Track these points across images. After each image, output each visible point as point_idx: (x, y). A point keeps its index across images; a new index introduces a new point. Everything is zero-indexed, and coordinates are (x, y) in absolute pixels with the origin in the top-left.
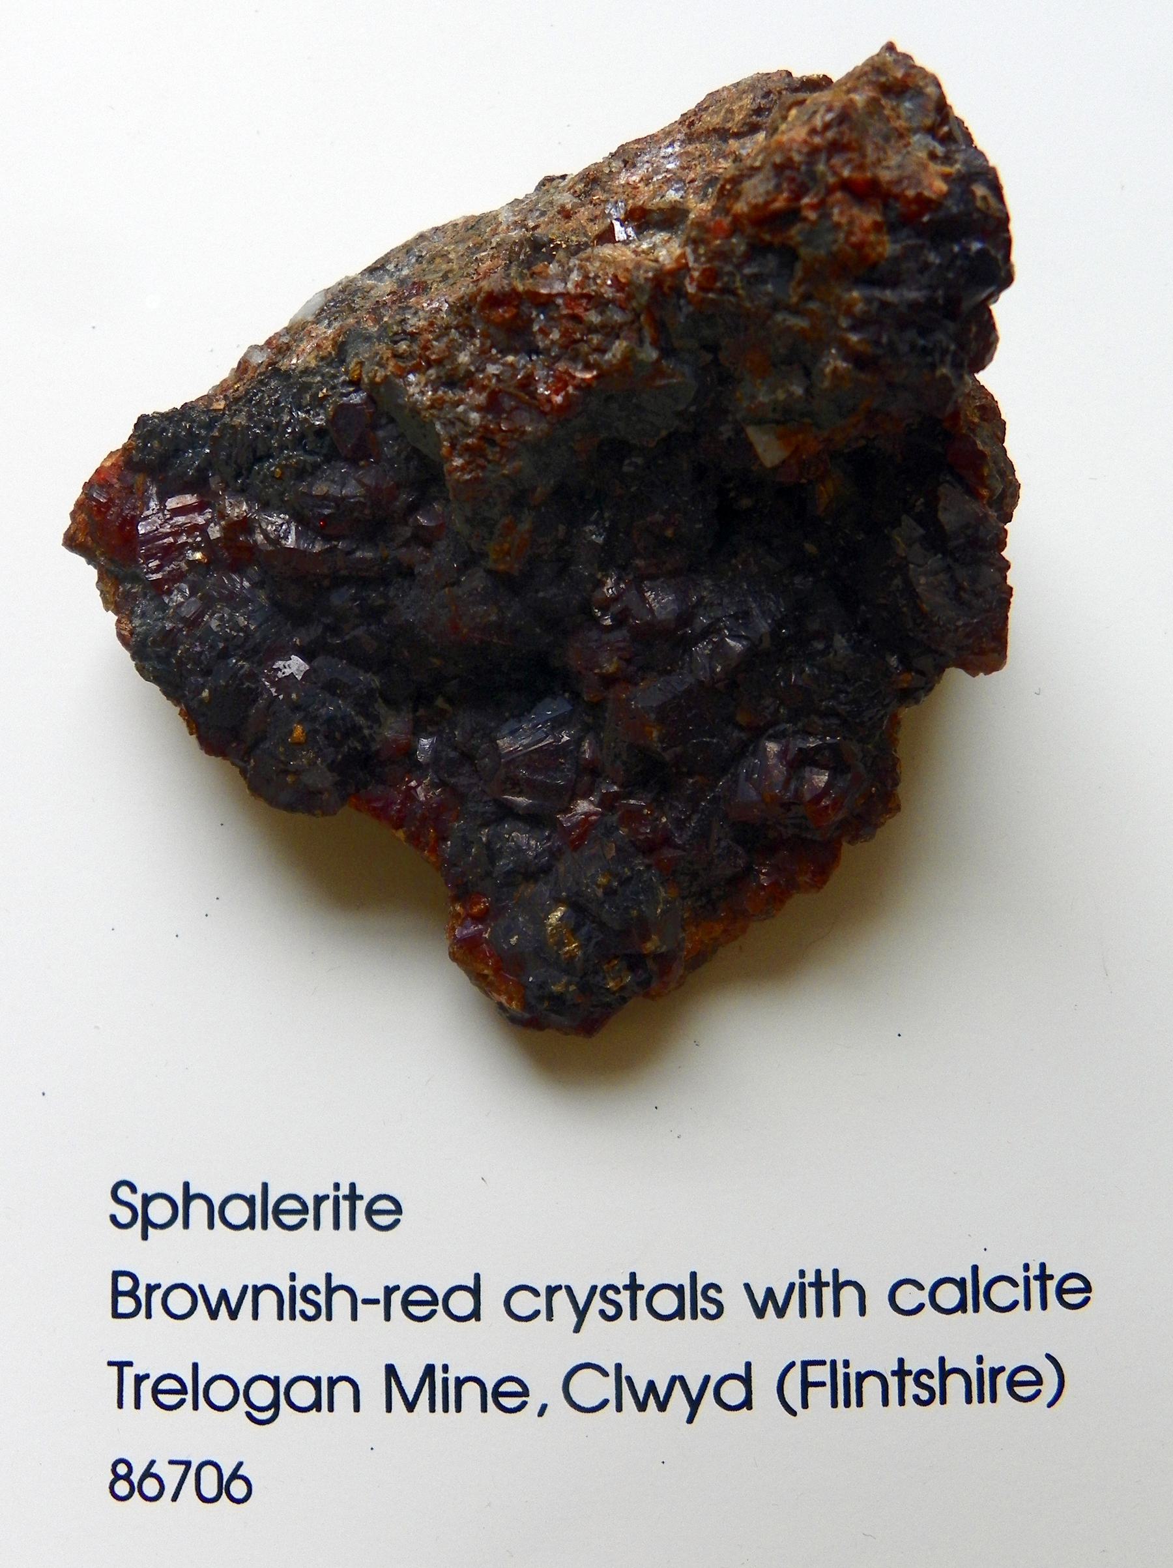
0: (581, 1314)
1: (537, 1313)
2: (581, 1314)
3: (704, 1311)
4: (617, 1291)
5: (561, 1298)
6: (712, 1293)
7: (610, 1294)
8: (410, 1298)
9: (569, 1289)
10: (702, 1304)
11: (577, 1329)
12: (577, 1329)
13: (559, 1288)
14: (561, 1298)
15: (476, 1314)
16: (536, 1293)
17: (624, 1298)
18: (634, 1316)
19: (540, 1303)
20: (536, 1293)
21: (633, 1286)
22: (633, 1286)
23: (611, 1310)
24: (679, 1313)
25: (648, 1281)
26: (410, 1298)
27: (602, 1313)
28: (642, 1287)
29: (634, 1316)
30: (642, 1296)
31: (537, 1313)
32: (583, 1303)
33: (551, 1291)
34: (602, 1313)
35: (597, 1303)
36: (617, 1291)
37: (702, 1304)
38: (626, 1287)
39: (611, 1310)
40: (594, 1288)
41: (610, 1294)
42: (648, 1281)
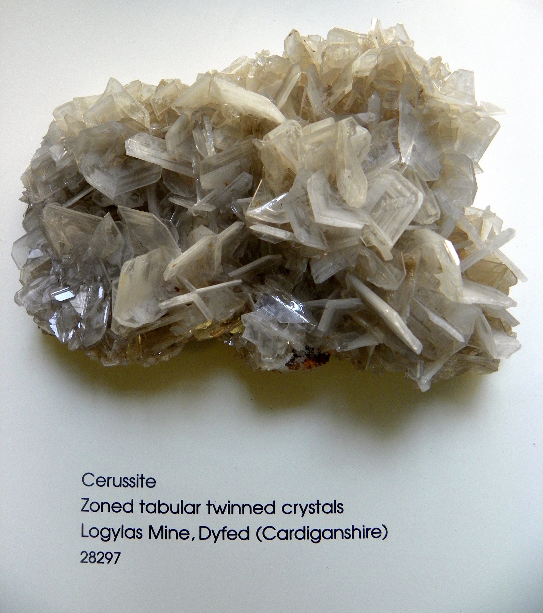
0: (304, 512)
1: (291, 512)
2: (304, 512)
3: (338, 511)
5: (298, 507)
6: (340, 506)
7: (312, 506)
9: (300, 505)
10: (337, 509)
11: (303, 516)
12: (303, 516)
13: (297, 504)
14: (298, 507)
16: (291, 506)
17: (316, 507)
18: (318, 512)
19: (292, 509)
20: (291, 506)
21: (318, 504)
22: (318, 504)
23: (312, 511)
24: (331, 512)
25: (322, 503)
27: (310, 512)
28: (321, 504)
29: (318, 512)
30: (321, 507)
31: (291, 512)
34: (310, 512)
35: (308, 509)
36: (314, 505)
37: (337, 509)
38: (316, 504)
39: (312, 511)
40: (307, 505)
41: (312, 506)
42: (322, 503)
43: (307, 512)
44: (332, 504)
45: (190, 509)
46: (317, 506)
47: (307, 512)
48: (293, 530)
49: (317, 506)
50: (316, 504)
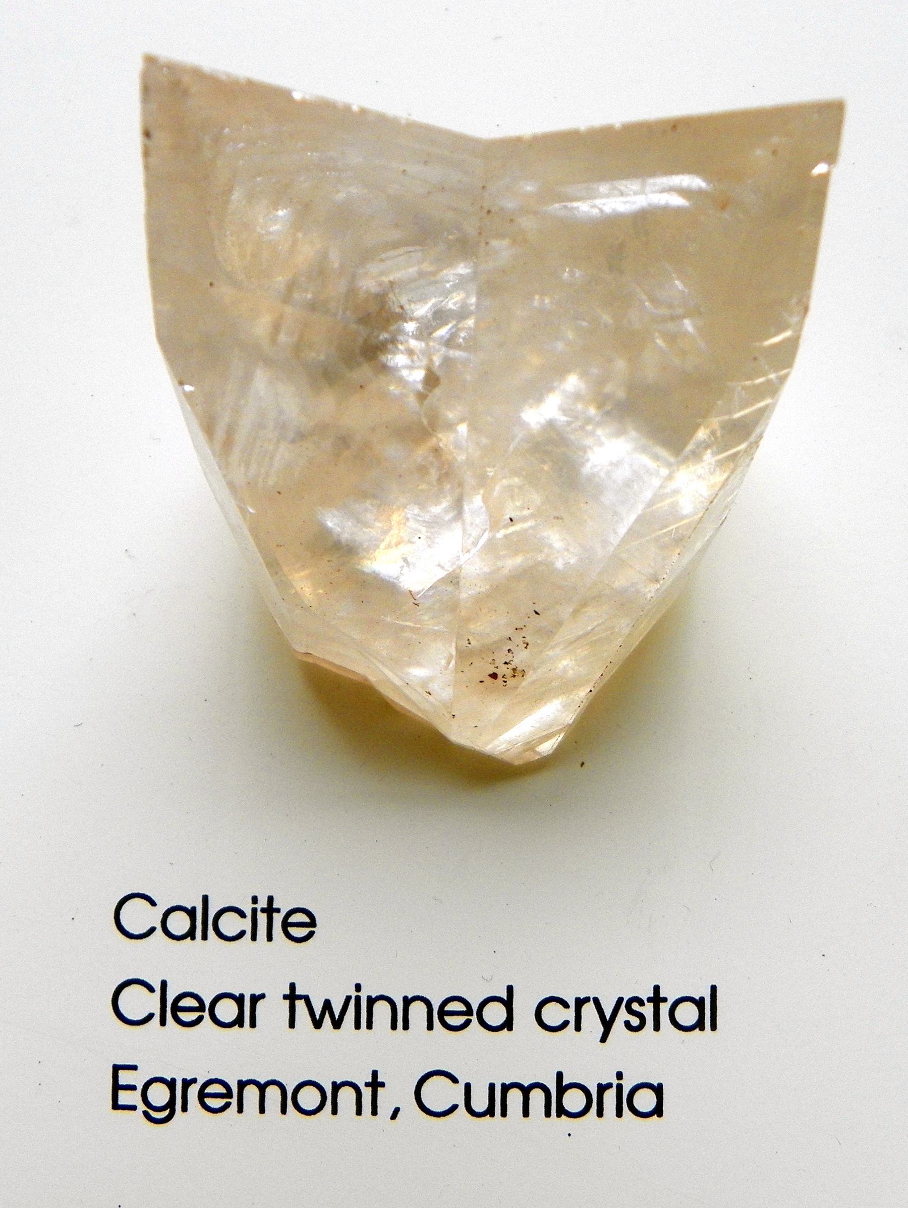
0: (608, 1025)
1: (566, 1024)
2: (608, 1025)
4: (641, 1003)
5: (589, 1010)
7: (635, 1006)
8: (446, 1008)
9: (597, 1002)
11: (604, 1039)
12: (604, 1039)
13: (587, 1000)
14: (589, 1010)
15: (508, 1024)
16: (566, 1005)
17: (648, 1010)
18: (657, 1027)
19: (569, 1014)
20: (566, 1005)
21: (657, 999)
22: (657, 999)
23: (635, 1022)
26: (446, 1008)
27: (628, 1024)
28: (665, 1000)
29: (657, 1027)
30: (664, 1008)
32: (609, 1015)
33: (580, 1003)
34: (628, 1024)
35: (623, 1015)
36: (641, 1003)
38: (649, 1000)
39: (635, 1022)
40: (620, 1000)
41: (635, 1006)
43: (619, 1024)
44: (702, 999)
45: (227, 1011)
46: (651, 1005)
47: (618, 1026)
48: (194, 1081)
49: (651, 1005)
50: (649, 1000)
